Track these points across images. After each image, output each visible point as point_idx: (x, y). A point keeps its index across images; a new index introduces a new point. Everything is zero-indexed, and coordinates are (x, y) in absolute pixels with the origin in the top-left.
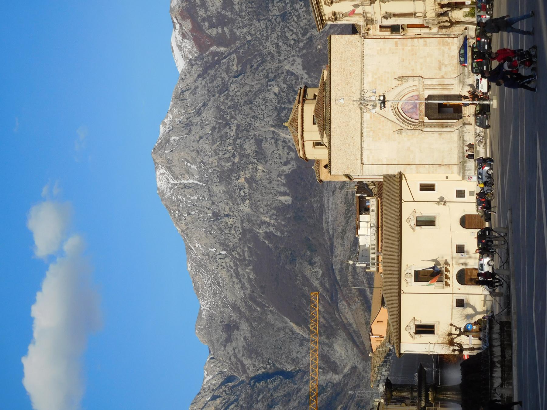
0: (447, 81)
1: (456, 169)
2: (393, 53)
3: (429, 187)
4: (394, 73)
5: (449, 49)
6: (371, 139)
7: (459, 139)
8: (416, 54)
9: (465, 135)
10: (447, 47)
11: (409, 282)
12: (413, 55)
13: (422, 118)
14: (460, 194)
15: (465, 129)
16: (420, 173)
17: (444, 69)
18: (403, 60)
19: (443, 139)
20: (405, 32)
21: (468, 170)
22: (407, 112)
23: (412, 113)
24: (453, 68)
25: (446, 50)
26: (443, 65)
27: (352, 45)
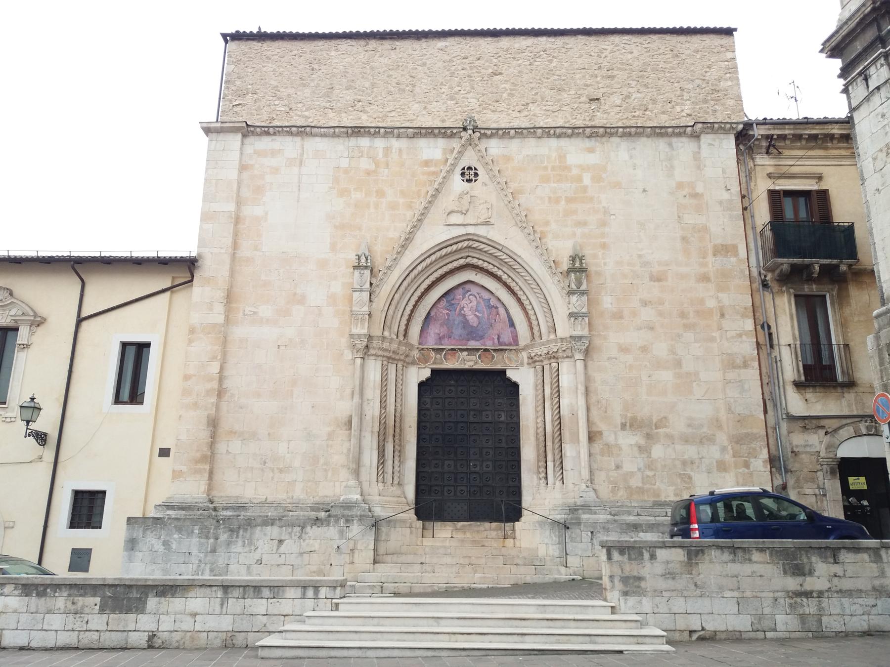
0: (575, 452)
1: (193, 490)
2: (684, 239)
3: (130, 386)
4: (604, 246)
6: (344, 163)
7: (315, 508)
8: (688, 327)
9: (332, 531)
10: (728, 457)
12: (683, 315)
13: (424, 360)
14: (87, 508)
15: (356, 529)
16: (190, 341)
17: (628, 440)
18: (657, 278)
19: (330, 436)
20: (775, 286)
21: (166, 544)
22: (451, 306)
23: (447, 323)
24: (636, 482)
25: (714, 453)
26: (648, 436)
27: (705, 101)
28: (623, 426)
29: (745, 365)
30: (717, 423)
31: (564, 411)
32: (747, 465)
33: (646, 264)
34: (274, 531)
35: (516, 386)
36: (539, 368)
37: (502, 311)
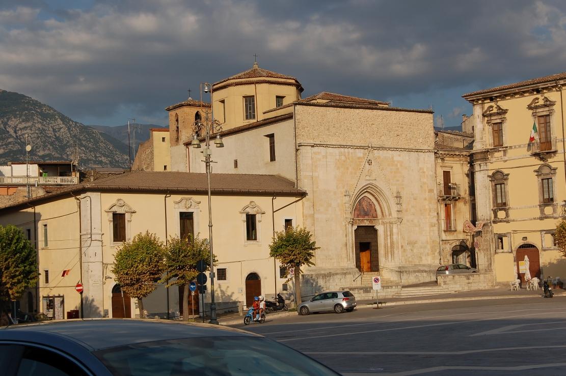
0: (398, 253)
5: (428, 254)
6: (338, 157)
11: (180, 204)
12: (421, 211)
19: (341, 248)
24: (410, 259)
26: (413, 246)
28: (408, 244)
29: (434, 226)
30: (427, 242)
31: (395, 240)
32: (434, 254)
33: (413, 194)
34: (339, 276)
35: (376, 231)
36: (385, 226)
37: (373, 206)
